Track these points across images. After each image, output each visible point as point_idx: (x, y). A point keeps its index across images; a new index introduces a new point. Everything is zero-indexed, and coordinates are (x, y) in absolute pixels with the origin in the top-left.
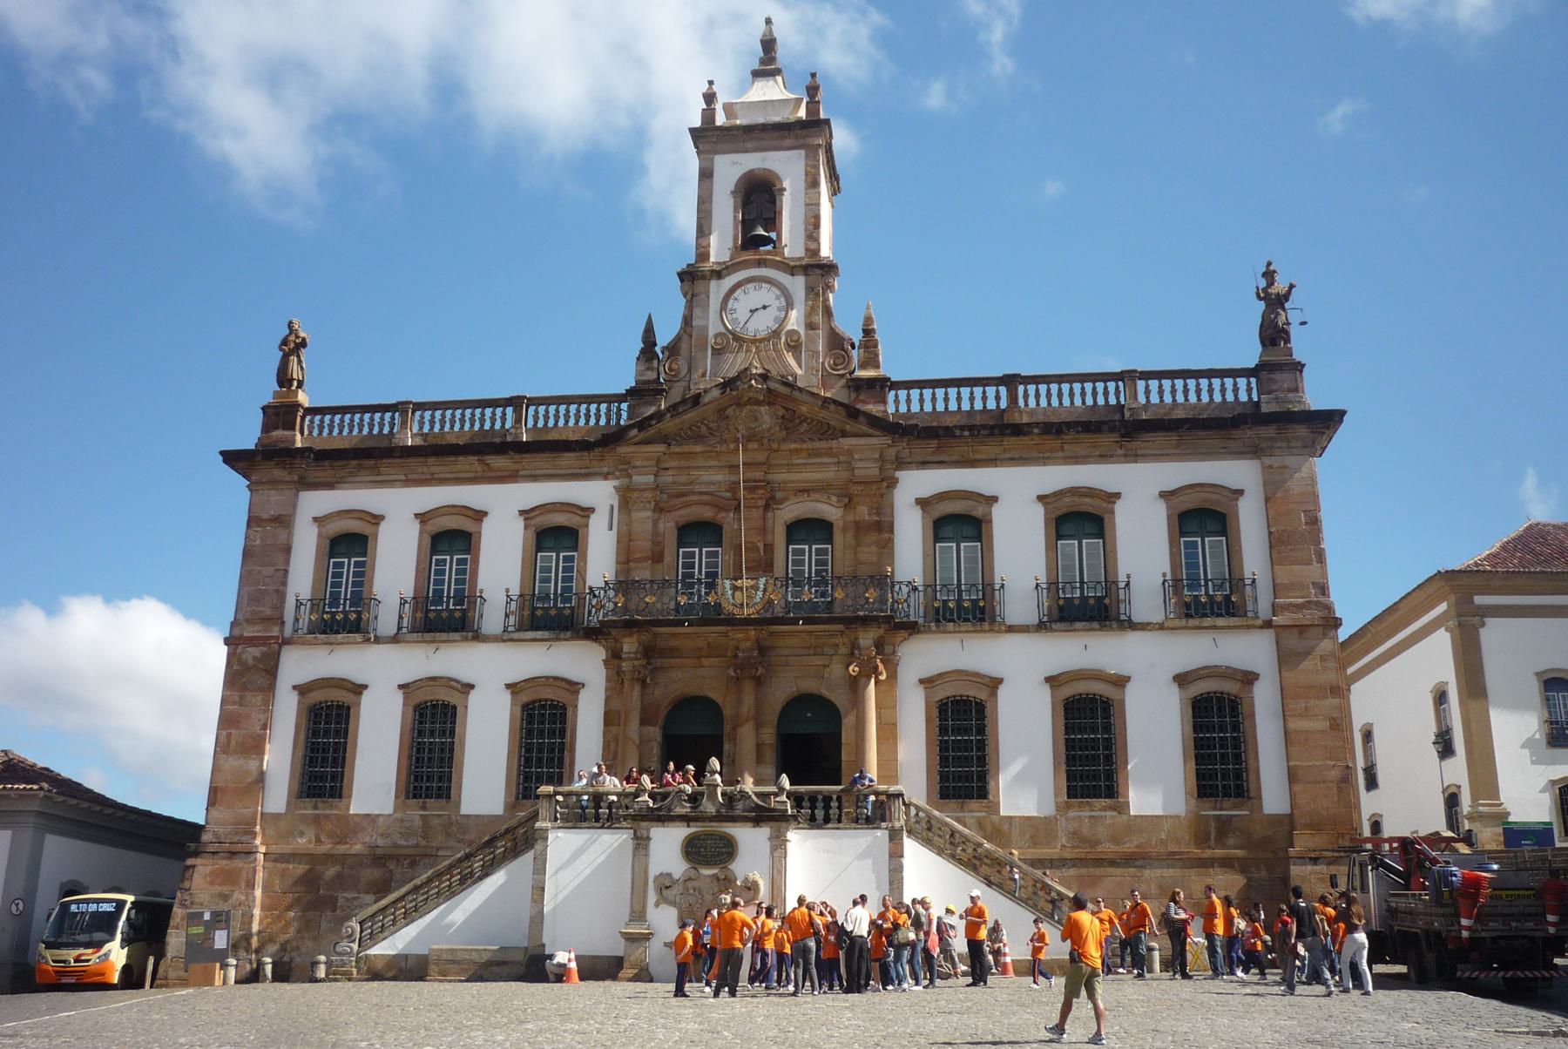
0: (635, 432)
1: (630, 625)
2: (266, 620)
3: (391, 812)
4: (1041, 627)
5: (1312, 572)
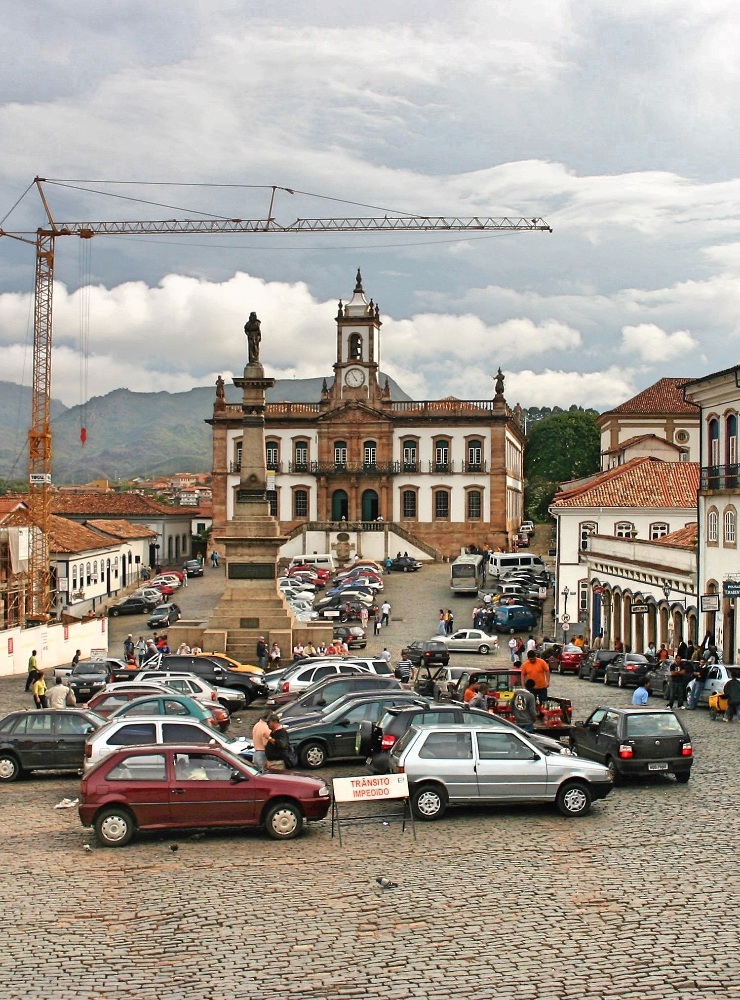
1: (323, 474)
4: (430, 474)
5: (501, 460)
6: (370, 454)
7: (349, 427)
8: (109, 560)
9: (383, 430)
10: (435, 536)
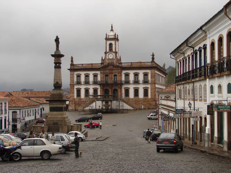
4: (133, 84)
6: (116, 78)
8: (35, 110)
10: (134, 102)
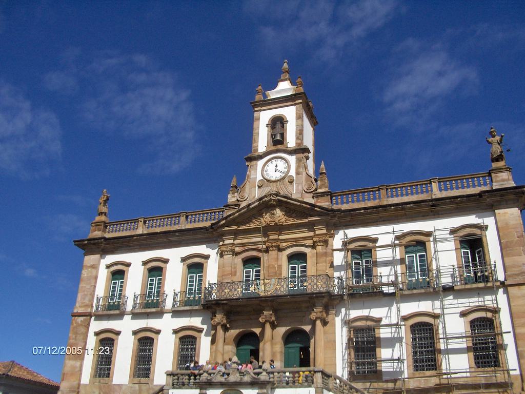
0: (224, 221)
2: (87, 306)
3: (127, 383)
7: (265, 235)
9: (317, 232)
